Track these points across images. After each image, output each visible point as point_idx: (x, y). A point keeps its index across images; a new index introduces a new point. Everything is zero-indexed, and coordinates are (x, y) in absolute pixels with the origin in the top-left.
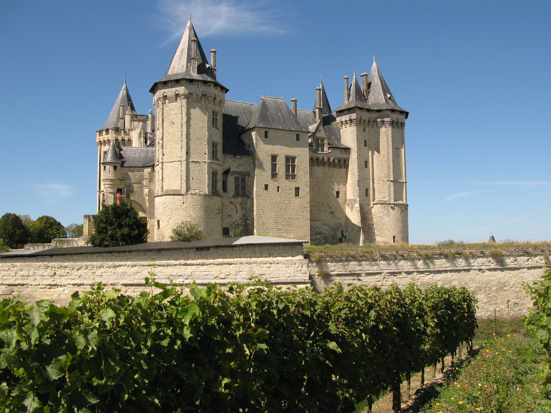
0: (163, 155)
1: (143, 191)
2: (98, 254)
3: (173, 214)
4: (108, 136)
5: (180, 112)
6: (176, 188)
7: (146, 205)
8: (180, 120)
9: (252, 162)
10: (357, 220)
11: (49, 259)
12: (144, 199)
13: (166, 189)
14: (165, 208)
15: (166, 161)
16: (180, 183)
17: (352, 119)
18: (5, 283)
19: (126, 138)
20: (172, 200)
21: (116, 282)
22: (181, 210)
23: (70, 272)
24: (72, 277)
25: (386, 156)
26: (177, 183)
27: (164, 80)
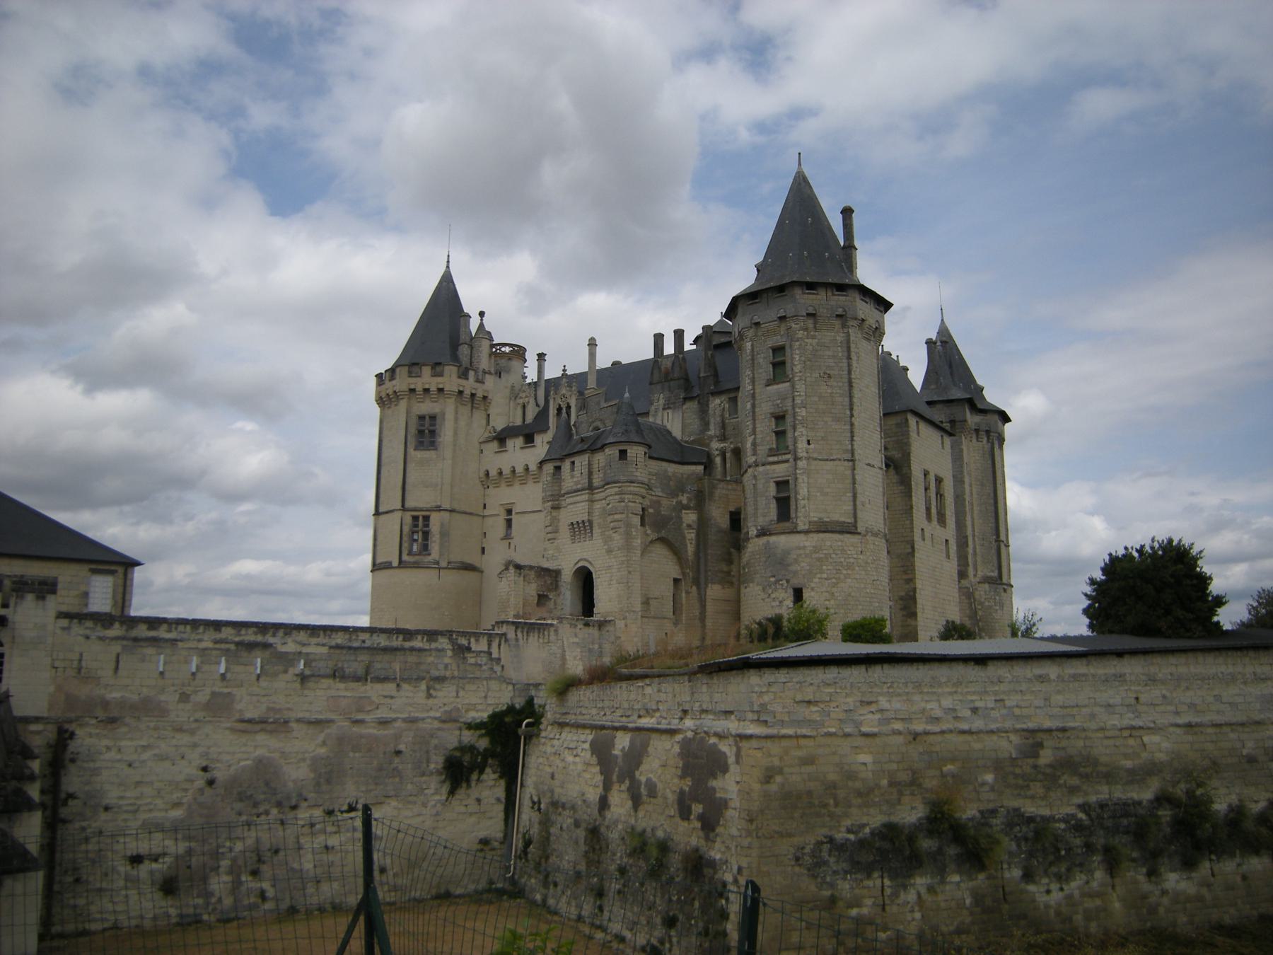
0: (809, 443)
1: (681, 518)
2: (1217, 653)
3: (842, 576)
4: (439, 379)
5: (846, 354)
6: (842, 519)
7: (687, 551)
8: (846, 372)
9: (895, 481)
10: (968, 612)
11: (1115, 663)
12: (684, 538)
13: (816, 519)
14: (819, 559)
15: (815, 455)
16: (851, 508)
17: (957, 419)
18: (1024, 726)
19: (480, 394)
20: (840, 543)
21: (1262, 716)
22: (857, 568)
23: (1168, 694)
24: (1172, 708)
25: (992, 495)
26: (845, 508)
27: (808, 279)
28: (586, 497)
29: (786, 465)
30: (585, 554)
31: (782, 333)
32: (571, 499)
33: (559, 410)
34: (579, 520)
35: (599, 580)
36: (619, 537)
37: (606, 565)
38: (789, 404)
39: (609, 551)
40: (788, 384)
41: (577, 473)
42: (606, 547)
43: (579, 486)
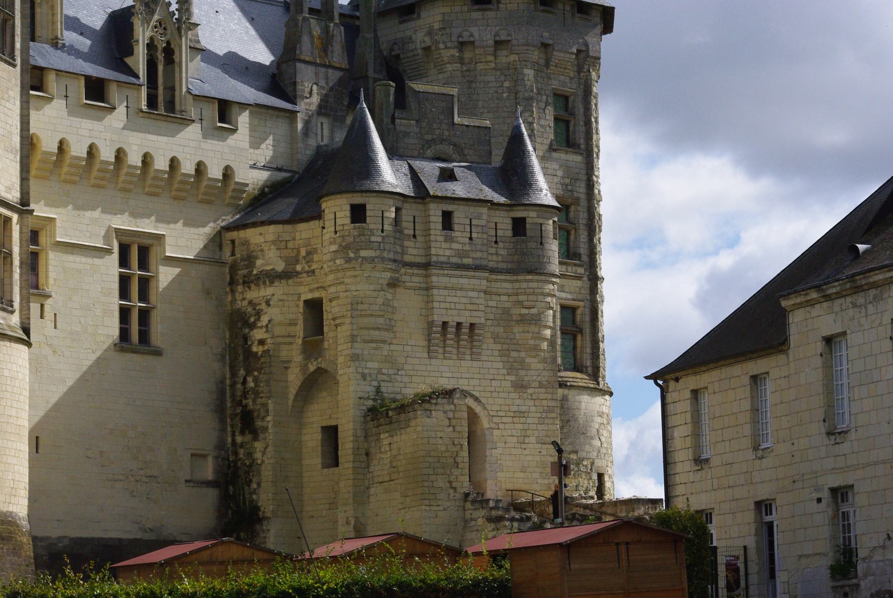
28: (484, 282)
29: (578, 283)
30: (465, 382)
31: (572, 75)
32: (446, 279)
33: (151, 46)
34: (465, 319)
35: (496, 432)
36: (541, 366)
37: (515, 408)
38: (581, 189)
39: (520, 386)
40: (579, 158)
41: (460, 233)
42: (513, 378)
43: (466, 261)
